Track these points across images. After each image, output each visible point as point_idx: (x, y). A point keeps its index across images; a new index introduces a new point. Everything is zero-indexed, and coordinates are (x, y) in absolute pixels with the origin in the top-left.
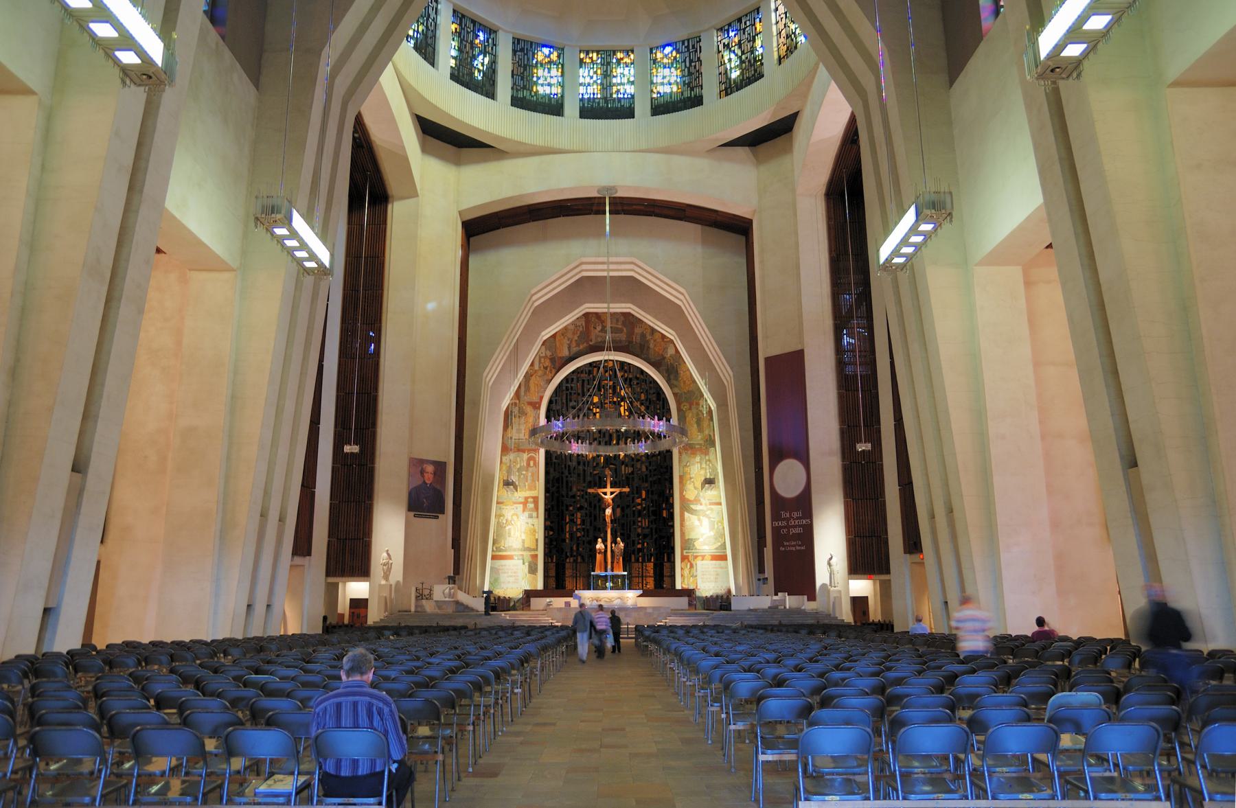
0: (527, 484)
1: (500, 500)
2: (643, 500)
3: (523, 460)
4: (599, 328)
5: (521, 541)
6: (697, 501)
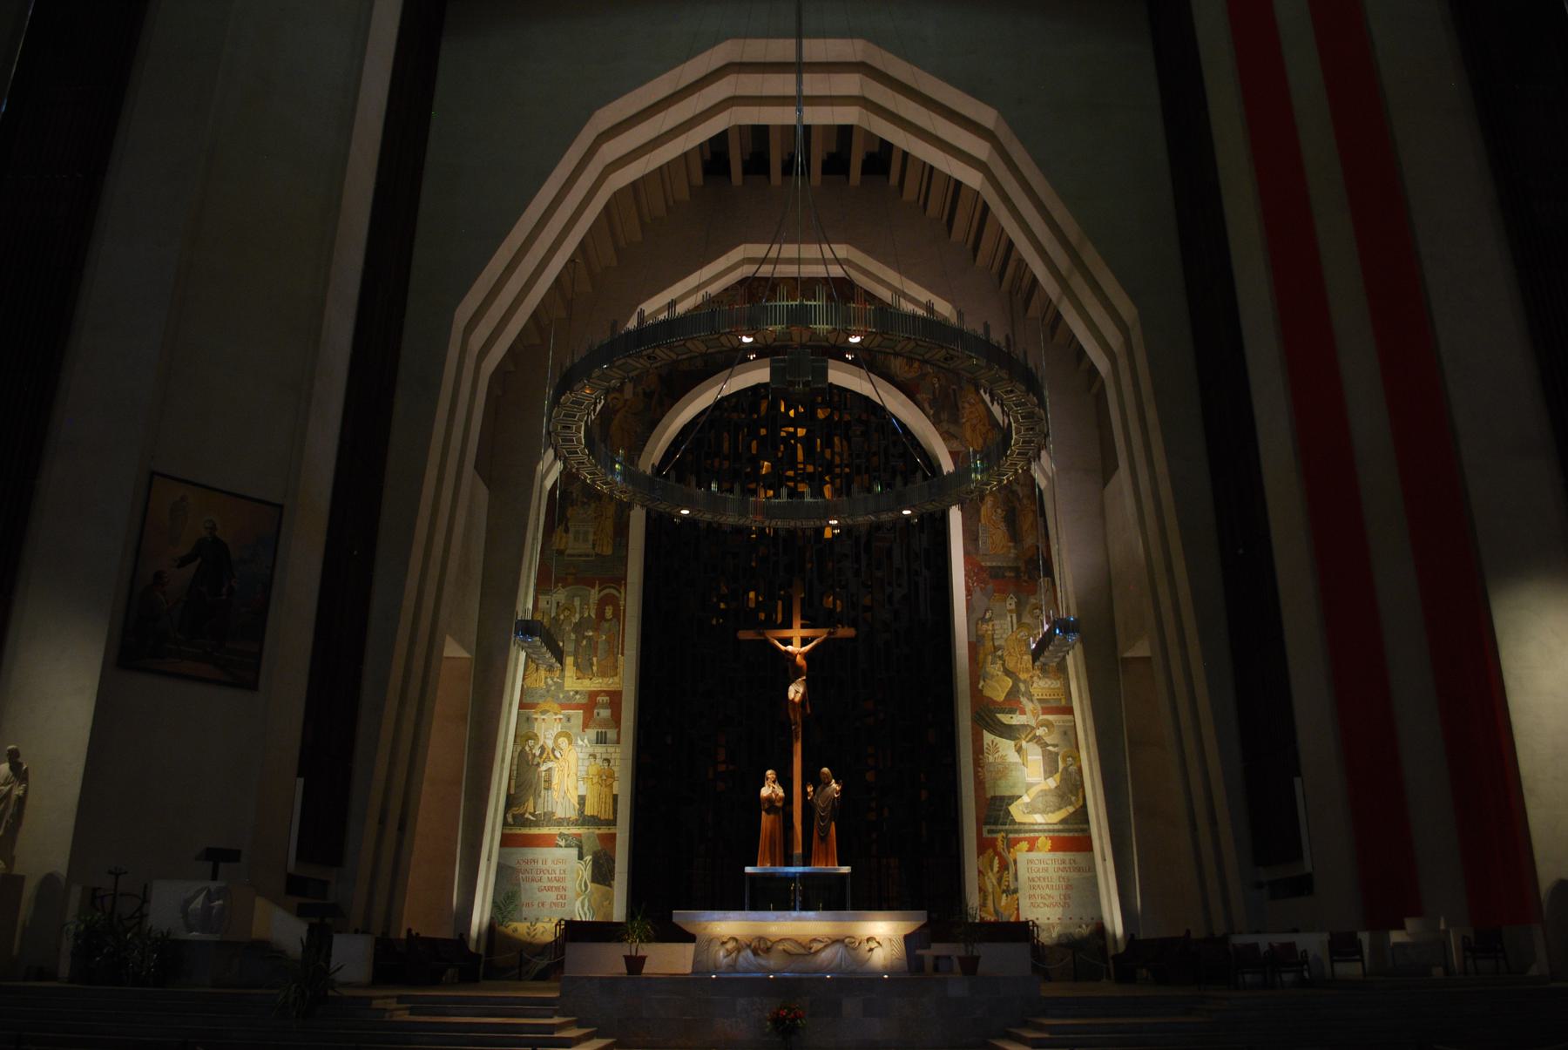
0: (595, 659)
1: (528, 700)
3: (588, 605)
5: (575, 801)
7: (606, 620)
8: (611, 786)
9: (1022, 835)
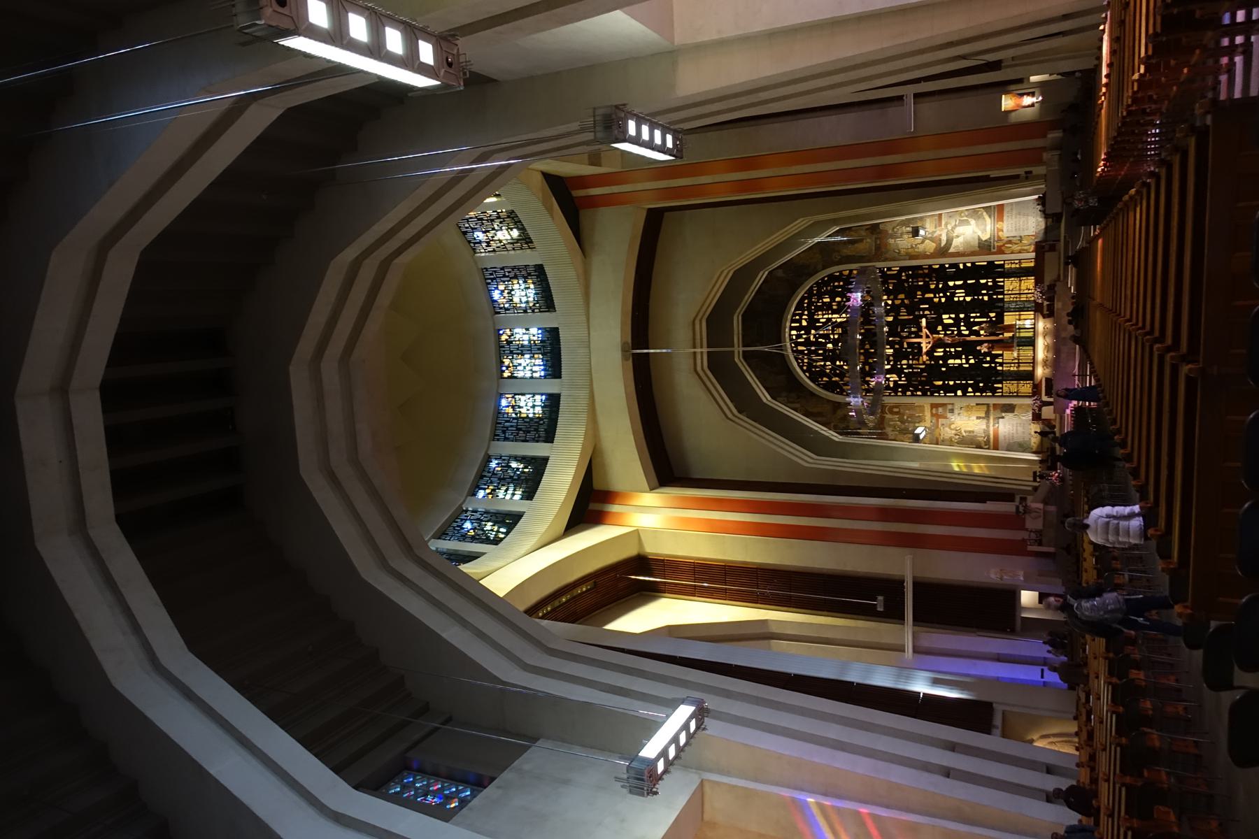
1: (935, 442)
2: (935, 297)
5: (979, 421)
6: (937, 240)
7: (900, 411)
8: (972, 406)
9: (996, 235)
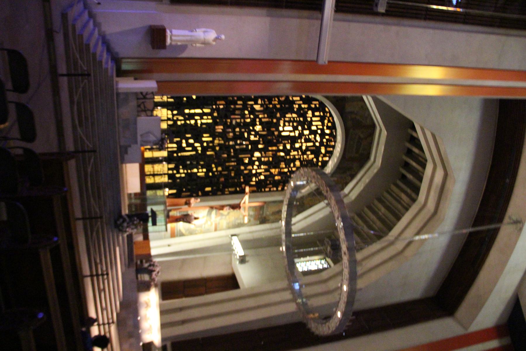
2: (220, 172)
4: (362, 136)
